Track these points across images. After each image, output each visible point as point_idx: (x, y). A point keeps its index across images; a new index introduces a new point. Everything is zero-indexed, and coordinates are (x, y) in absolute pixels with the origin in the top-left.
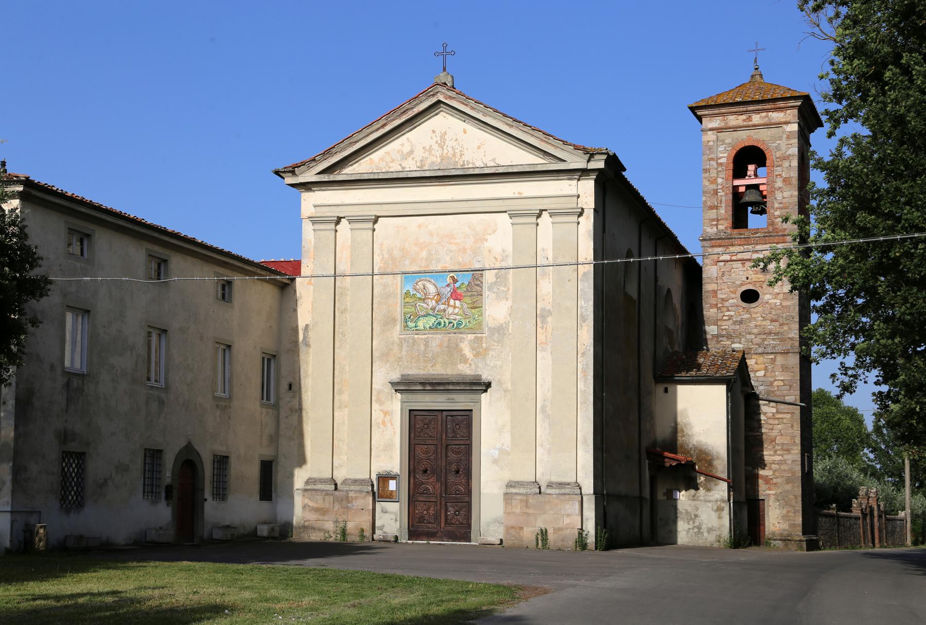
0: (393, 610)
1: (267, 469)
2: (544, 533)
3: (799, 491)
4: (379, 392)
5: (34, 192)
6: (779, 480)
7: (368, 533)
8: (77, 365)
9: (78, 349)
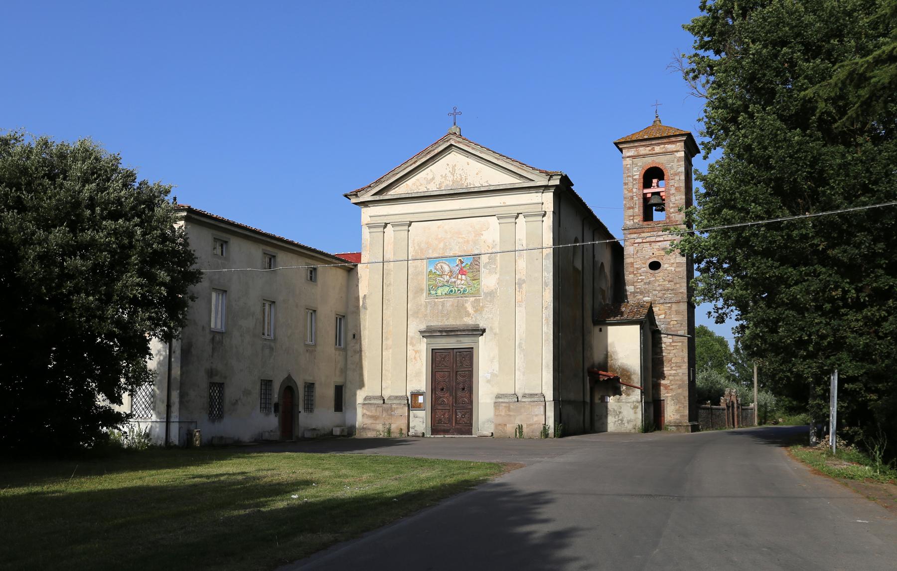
0: (421, 481)
1: (339, 391)
2: (520, 428)
3: (686, 393)
4: (412, 338)
5: (193, 216)
6: (673, 387)
7: (405, 432)
8: (219, 327)
9: (220, 316)
